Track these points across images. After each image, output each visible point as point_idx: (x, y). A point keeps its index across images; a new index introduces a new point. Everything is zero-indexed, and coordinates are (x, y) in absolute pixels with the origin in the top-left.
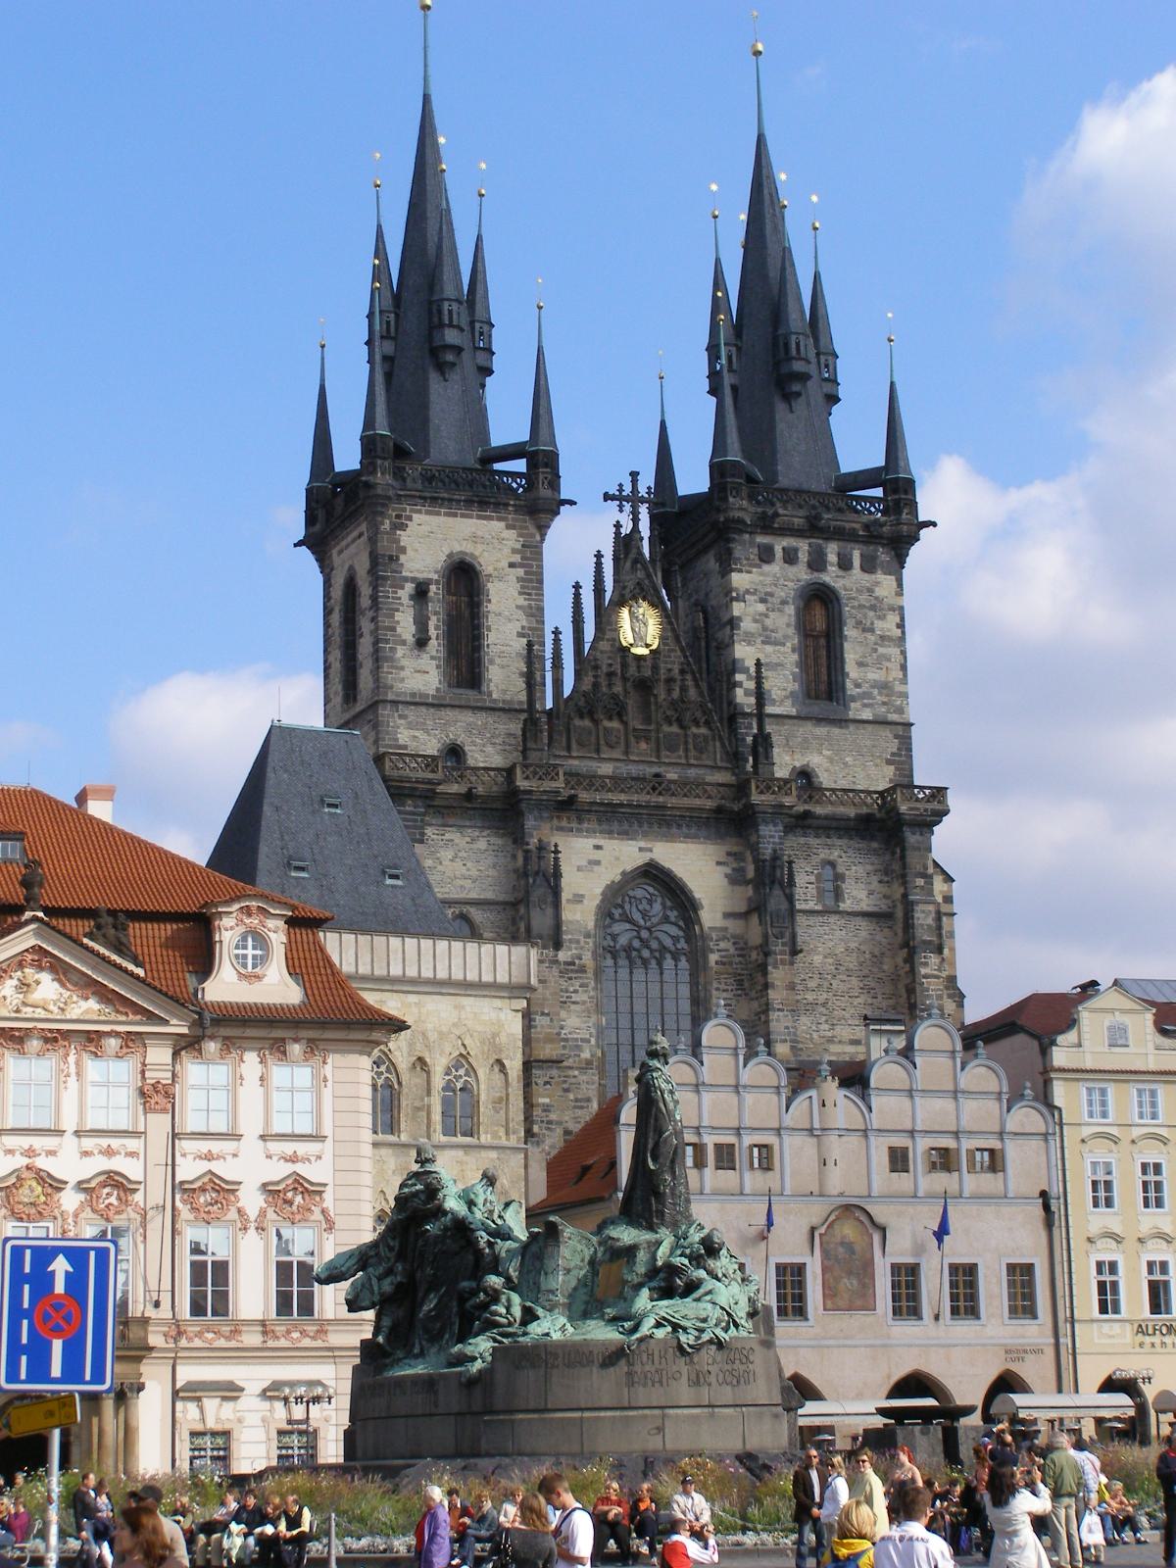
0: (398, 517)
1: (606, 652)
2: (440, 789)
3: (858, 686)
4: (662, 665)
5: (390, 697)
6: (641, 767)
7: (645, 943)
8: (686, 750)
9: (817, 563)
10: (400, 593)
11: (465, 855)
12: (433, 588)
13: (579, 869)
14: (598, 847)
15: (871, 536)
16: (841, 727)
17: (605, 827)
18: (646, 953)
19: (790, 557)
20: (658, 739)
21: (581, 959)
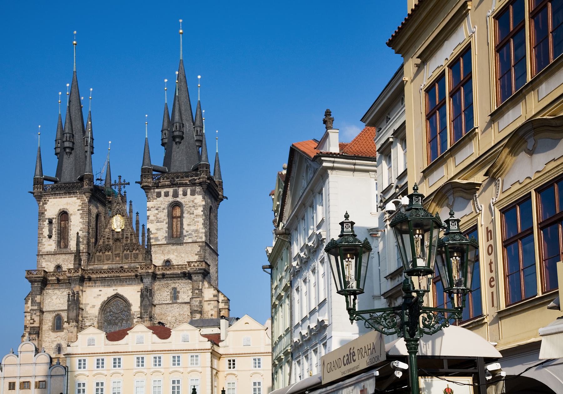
0: (45, 201)
1: (108, 232)
2: (50, 278)
3: (187, 232)
4: (125, 234)
5: (41, 253)
6: (116, 265)
7: (117, 318)
8: (131, 258)
9: (176, 195)
10: (45, 223)
11: (59, 297)
12: (54, 221)
13: (94, 298)
14: (100, 291)
15: (193, 184)
16: (181, 245)
17: (103, 284)
18: (117, 321)
19: (167, 195)
20: (122, 256)
21: (93, 324)
